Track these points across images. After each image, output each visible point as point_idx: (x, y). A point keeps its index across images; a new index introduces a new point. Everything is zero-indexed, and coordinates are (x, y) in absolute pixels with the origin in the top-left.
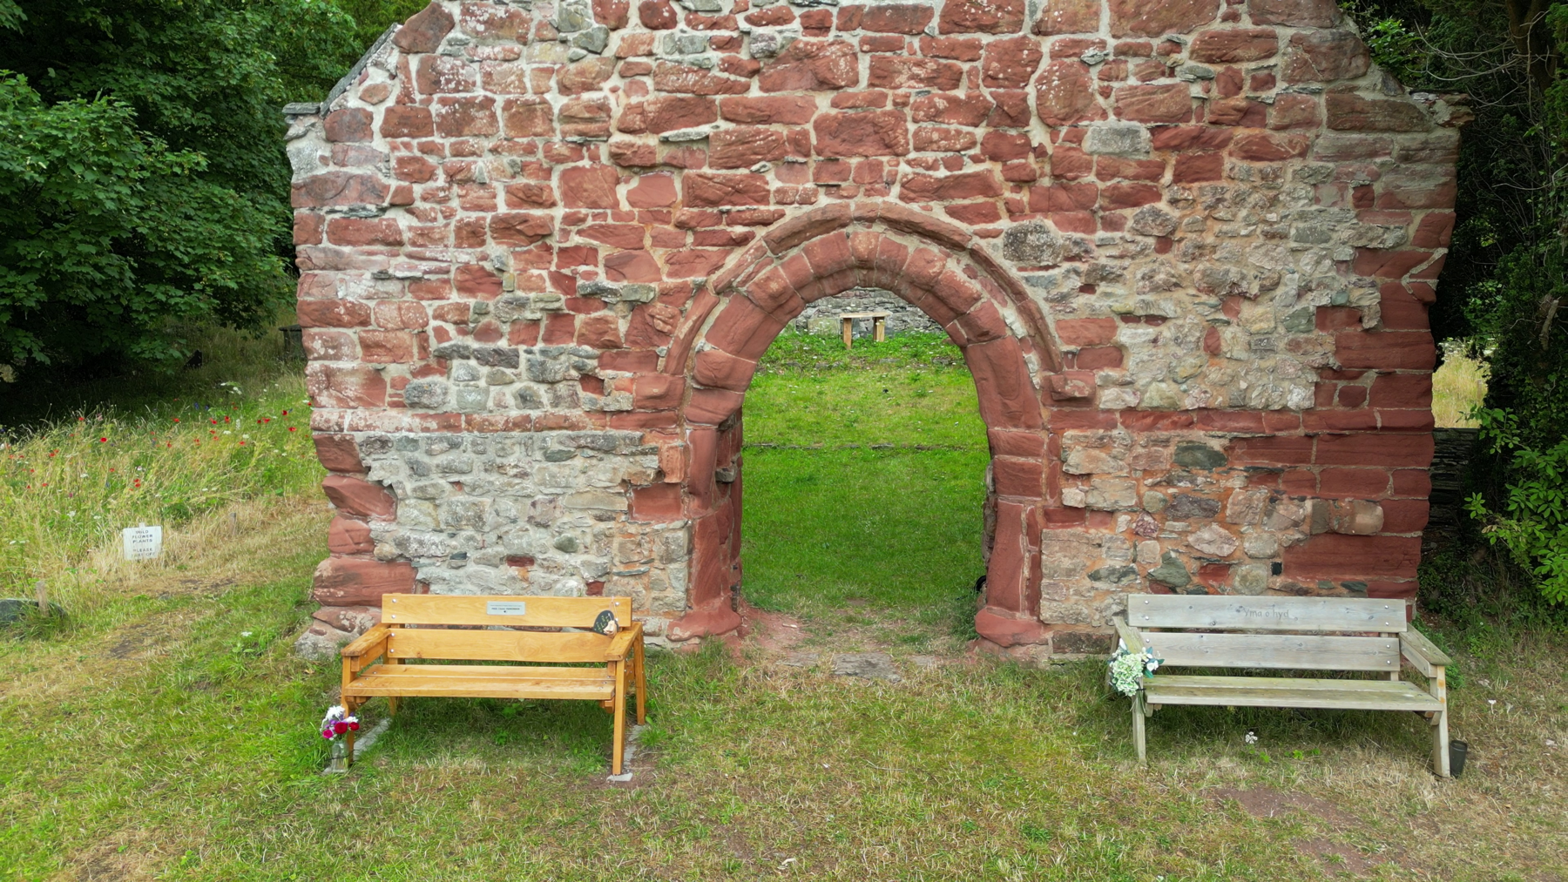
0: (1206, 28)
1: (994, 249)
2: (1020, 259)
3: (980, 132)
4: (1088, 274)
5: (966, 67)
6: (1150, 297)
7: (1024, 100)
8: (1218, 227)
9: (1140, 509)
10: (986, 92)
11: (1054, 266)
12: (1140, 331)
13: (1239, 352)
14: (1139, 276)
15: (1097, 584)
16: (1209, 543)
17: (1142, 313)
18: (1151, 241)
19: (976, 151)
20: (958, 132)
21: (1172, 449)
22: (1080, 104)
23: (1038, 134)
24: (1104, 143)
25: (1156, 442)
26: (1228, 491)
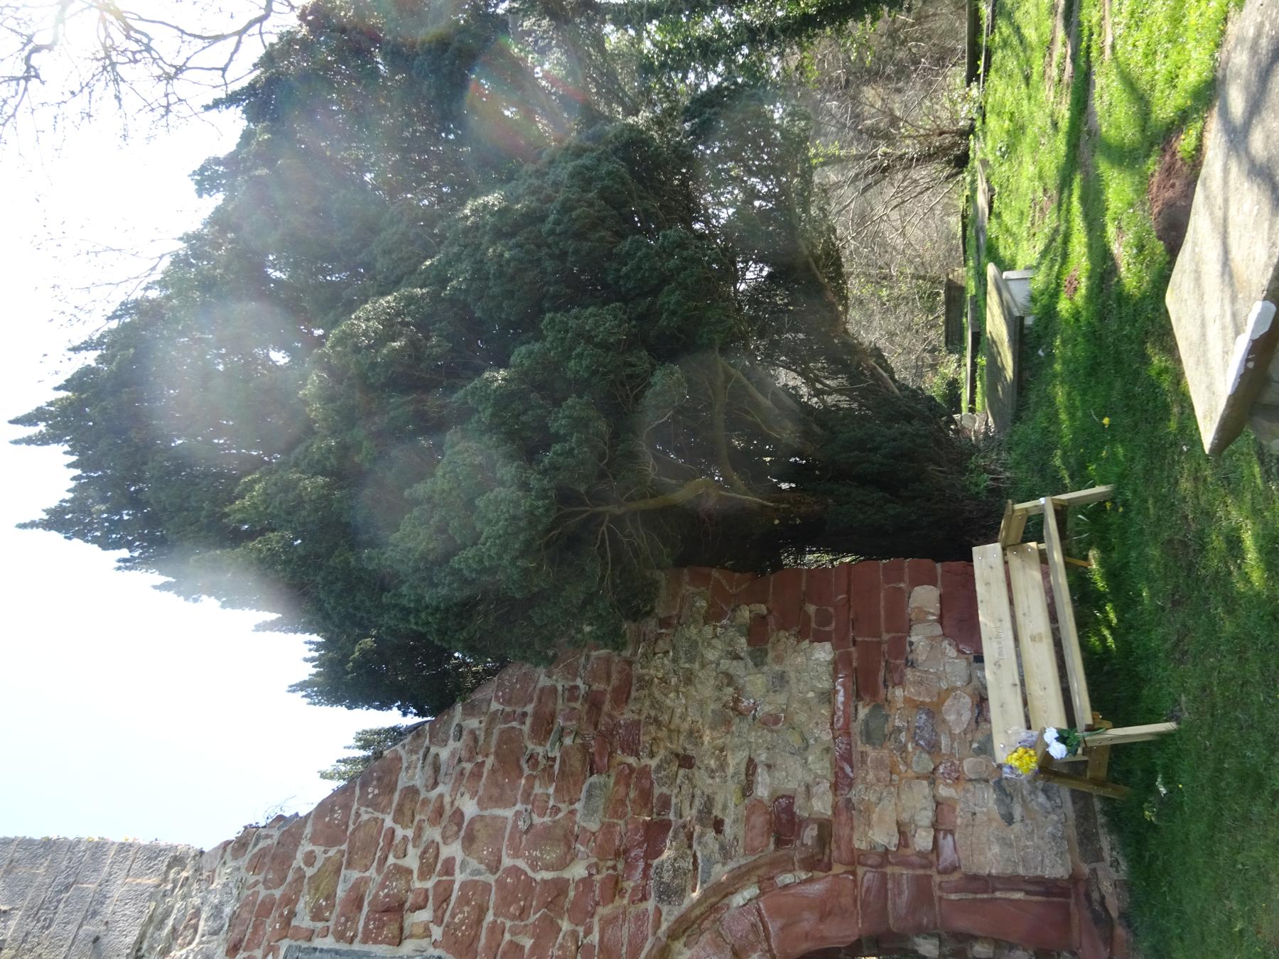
0: (526, 736)
1: (670, 914)
2: (683, 890)
3: (565, 925)
4: (703, 825)
5: (507, 936)
6: (731, 770)
7: (545, 882)
8: (676, 721)
9: (932, 778)
10: (533, 918)
11: (695, 856)
12: (760, 779)
13: (781, 699)
14: (710, 781)
15: (1017, 816)
16: (959, 714)
17: (743, 777)
18: (682, 772)
19: (581, 930)
20: (561, 947)
21: (868, 748)
22: (559, 832)
23: (578, 871)
24: (595, 811)
25: (864, 762)
26: (907, 700)
